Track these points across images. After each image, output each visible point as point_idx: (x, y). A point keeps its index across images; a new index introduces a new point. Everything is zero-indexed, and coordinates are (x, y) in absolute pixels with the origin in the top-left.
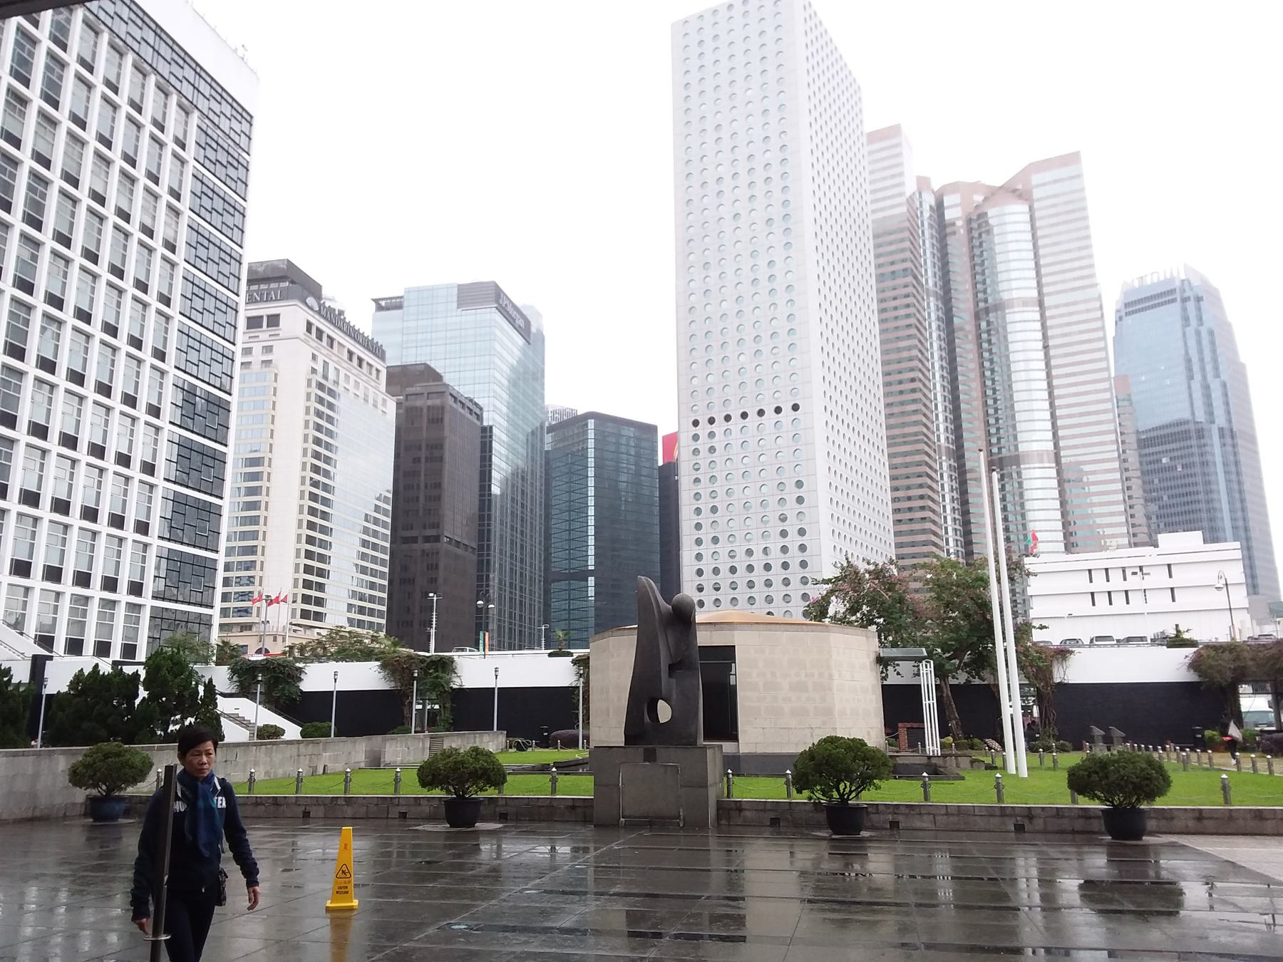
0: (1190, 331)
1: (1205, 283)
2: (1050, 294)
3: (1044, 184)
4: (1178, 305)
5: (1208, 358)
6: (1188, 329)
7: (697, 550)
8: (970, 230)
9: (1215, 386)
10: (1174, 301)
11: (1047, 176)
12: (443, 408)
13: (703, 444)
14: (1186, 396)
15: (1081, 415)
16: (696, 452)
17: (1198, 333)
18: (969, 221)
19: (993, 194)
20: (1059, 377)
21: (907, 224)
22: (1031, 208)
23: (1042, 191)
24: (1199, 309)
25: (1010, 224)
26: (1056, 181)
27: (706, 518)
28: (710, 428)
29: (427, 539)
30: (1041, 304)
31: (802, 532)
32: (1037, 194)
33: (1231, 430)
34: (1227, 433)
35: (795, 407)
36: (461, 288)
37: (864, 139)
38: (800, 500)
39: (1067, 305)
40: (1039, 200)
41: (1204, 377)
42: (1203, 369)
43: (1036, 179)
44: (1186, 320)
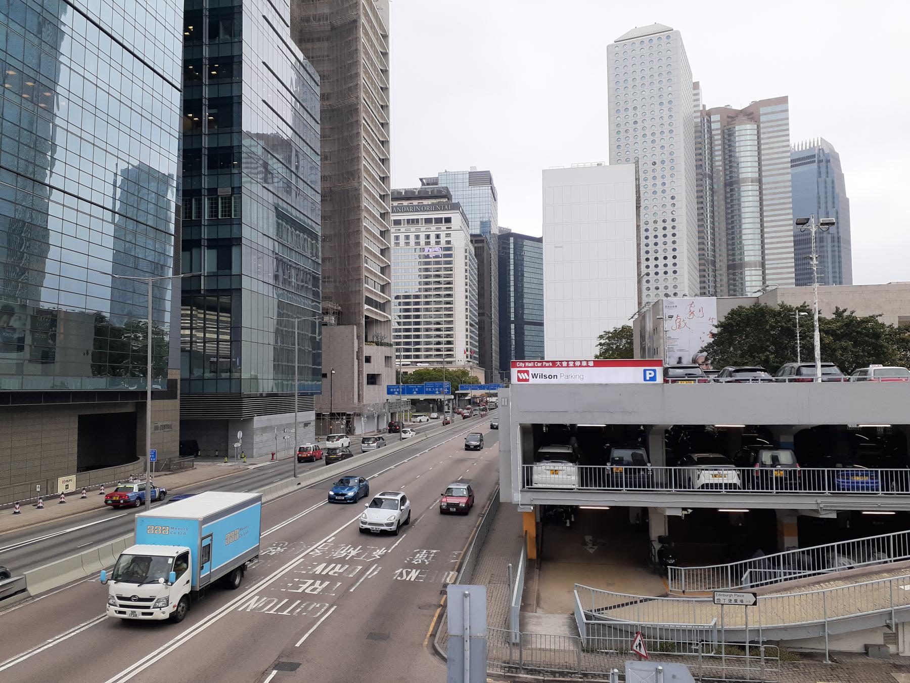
0: (821, 180)
1: (832, 150)
2: (766, 176)
6: (820, 180)
11: (769, 109)
15: (777, 243)
17: (825, 182)
20: (767, 222)
23: (765, 114)
25: (745, 134)
26: (773, 113)
32: (762, 119)
33: (839, 238)
34: (836, 240)
41: (826, 208)
44: (820, 173)
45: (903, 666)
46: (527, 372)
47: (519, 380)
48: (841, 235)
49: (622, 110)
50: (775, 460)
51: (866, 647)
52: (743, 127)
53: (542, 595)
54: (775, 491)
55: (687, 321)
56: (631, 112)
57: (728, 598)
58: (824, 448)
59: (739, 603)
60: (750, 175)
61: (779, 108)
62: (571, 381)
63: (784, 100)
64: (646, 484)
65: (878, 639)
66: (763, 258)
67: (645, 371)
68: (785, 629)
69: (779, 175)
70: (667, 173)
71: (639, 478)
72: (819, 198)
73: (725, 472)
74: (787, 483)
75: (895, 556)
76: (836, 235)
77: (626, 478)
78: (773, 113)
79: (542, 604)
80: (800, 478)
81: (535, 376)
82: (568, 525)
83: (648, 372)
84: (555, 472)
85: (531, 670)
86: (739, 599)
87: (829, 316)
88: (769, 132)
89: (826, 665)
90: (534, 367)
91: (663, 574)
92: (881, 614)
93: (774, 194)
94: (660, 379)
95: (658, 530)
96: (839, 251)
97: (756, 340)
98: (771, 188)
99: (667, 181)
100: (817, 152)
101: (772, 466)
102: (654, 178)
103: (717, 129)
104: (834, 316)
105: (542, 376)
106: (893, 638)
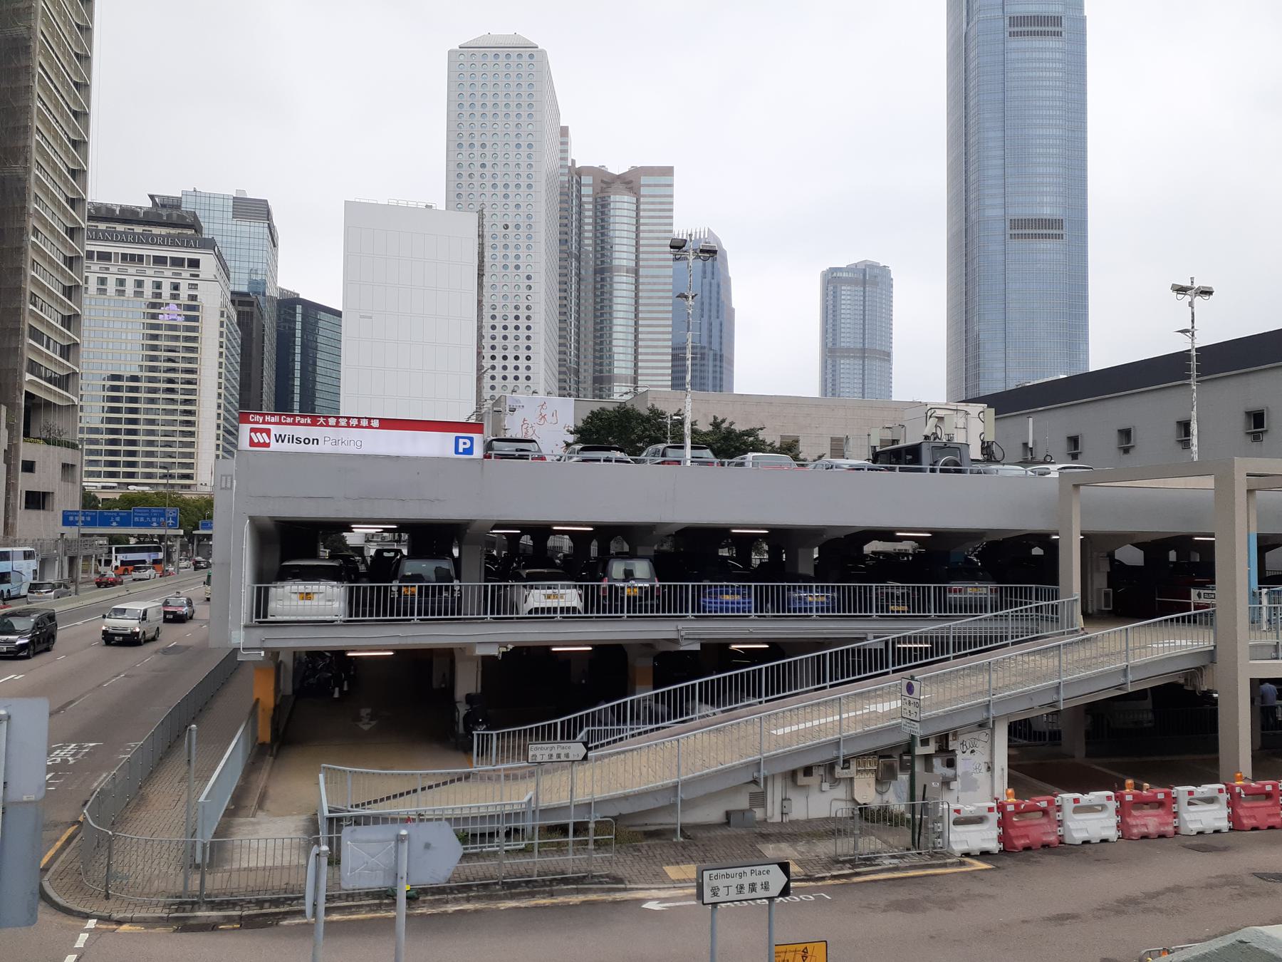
2: (644, 267)
3: (649, 186)
5: (714, 301)
9: (716, 323)
22: (638, 200)
25: (621, 204)
26: (656, 185)
30: (636, 272)
32: (643, 191)
33: (721, 356)
39: (653, 277)
40: (645, 196)
44: (704, 272)
45: (769, 835)
46: (268, 432)
47: (252, 443)
48: (724, 352)
49: (466, 145)
50: (629, 575)
51: (728, 814)
52: (618, 198)
53: (271, 792)
54: (625, 614)
55: (536, 427)
56: (477, 151)
57: (547, 753)
58: (694, 556)
59: (563, 758)
60: (624, 263)
61: (663, 180)
62: (342, 449)
63: (668, 171)
64: (450, 610)
65: (742, 802)
66: (636, 372)
67: (457, 439)
68: (626, 798)
70: (523, 242)
71: (440, 602)
73: (562, 591)
74: (641, 605)
75: (767, 695)
77: (420, 602)
78: (656, 185)
79: (268, 805)
80: (658, 597)
81: (280, 438)
82: (336, 695)
83: (461, 441)
84: (307, 596)
85: (221, 903)
86: (563, 752)
87: (705, 427)
89: (676, 844)
90: (280, 423)
91: (464, 747)
92: (747, 766)
93: (652, 291)
94: (478, 452)
95: (467, 683)
96: (721, 373)
97: (617, 432)
99: (523, 252)
101: (624, 581)
102: (506, 247)
103: (588, 196)
104: (711, 428)
105: (292, 439)
106: (759, 799)
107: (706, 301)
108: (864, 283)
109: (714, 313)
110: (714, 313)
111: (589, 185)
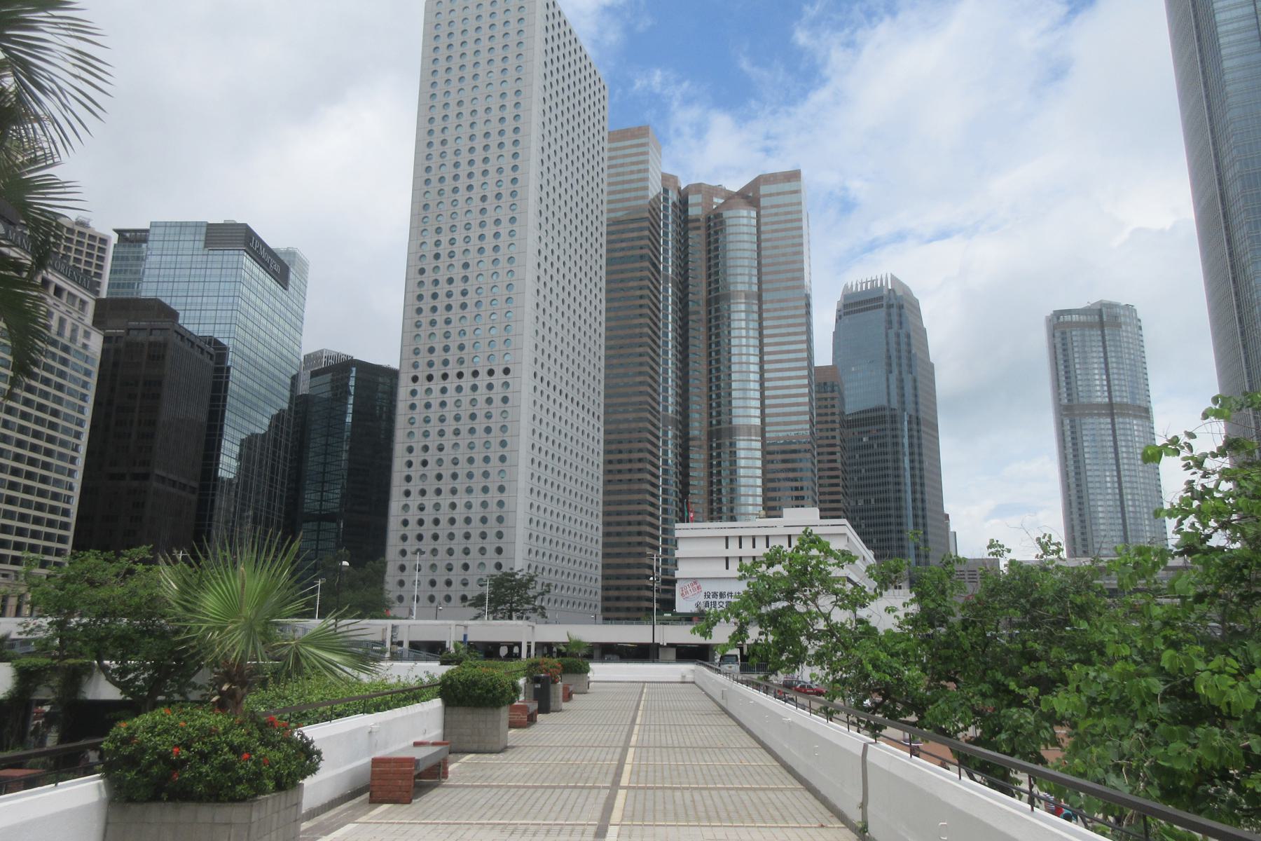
0: (892, 333)
4: (884, 309)
7: (404, 500)
8: (709, 227)
9: (908, 379)
10: (882, 306)
11: (773, 188)
12: (165, 345)
13: (420, 400)
14: (885, 386)
16: (413, 407)
17: (898, 335)
18: (709, 219)
19: (730, 197)
21: (647, 215)
22: (758, 214)
24: (900, 315)
26: (778, 194)
27: (416, 471)
28: (427, 385)
29: (136, 477)
31: (501, 489)
32: (764, 202)
34: (914, 420)
35: (507, 371)
36: (211, 228)
37: (606, 135)
38: (503, 459)
39: (780, 301)
41: (900, 373)
42: (900, 365)
43: (764, 189)
44: (890, 322)
48: (921, 415)
61: (787, 187)
63: (794, 175)
69: (787, 288)
72: (889, 357)
76: (913, 413)
78: (778, 194)
88: (773, 223)
96: (919, 438)
98: (775, 310)
100: (885, 292)
107: (894, 354)
108: (1102, 325)
109: (905, 368)
110: (905, 368)
111: (698, 204)
